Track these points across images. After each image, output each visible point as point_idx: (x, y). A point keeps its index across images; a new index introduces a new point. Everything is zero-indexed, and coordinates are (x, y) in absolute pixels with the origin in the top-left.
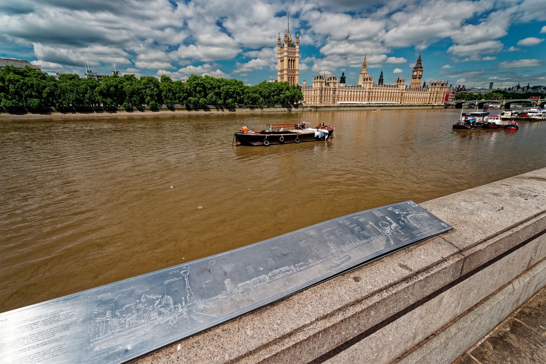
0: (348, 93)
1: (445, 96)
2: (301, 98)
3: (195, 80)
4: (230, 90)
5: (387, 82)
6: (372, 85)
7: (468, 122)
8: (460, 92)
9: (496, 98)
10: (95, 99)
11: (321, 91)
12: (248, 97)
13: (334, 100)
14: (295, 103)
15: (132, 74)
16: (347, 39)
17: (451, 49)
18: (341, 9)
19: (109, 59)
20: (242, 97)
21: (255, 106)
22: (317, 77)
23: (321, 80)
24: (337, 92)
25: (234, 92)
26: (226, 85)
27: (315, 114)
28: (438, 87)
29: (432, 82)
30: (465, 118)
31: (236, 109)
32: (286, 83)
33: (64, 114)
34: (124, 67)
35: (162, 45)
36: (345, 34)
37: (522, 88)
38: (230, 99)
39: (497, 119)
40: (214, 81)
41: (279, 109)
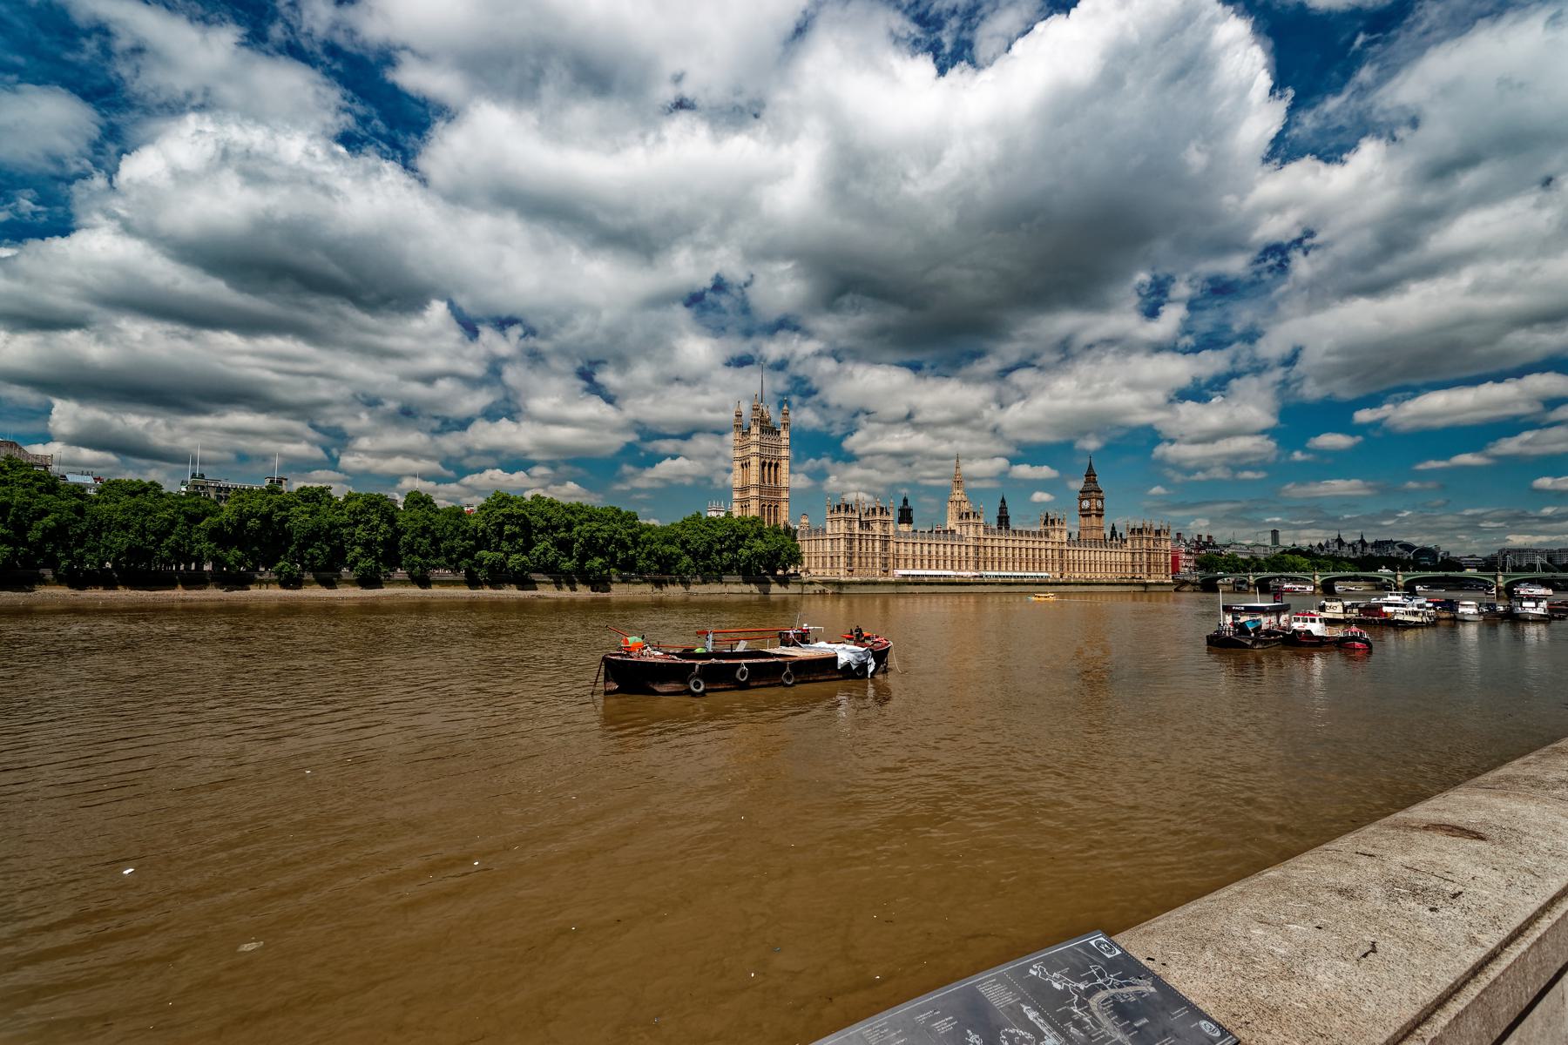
0: (922, 548)
1: (1170, 561)
2: (796, 558)
3: (504, 507)
4: (599, 534)
5: (1020, 524)
6: (981, 529)
7: (1242, 628)
8: (1204, 552)
9: (1294, 567)
10: (192, 549)
11: (851, 541)
12: (649, 555)
13: (886, 565)
14: (780, 572)
15: (324, 485)
16: (908, 419)
17: (1159, 450)
18: (890, 355)
19: (266, 445)
20: (630, 552)
21: (667, 577)
22: (839, 507)
23: (849, 515)
24: (892, 546)
25: (609, 541)
27: (835, 603)
28: (1148, 539)
29: (1131, 526)
30: (1233, 619)
31: (613, 587)
32: (755, 520)
33: (78, 592)
34: (303, 466)
35: (424, 417)
36: (903, 410)
37: (1349, 545)
38: (596, 558)
39: (1313, 621)
40: (557, 511)
41: (736, 588)
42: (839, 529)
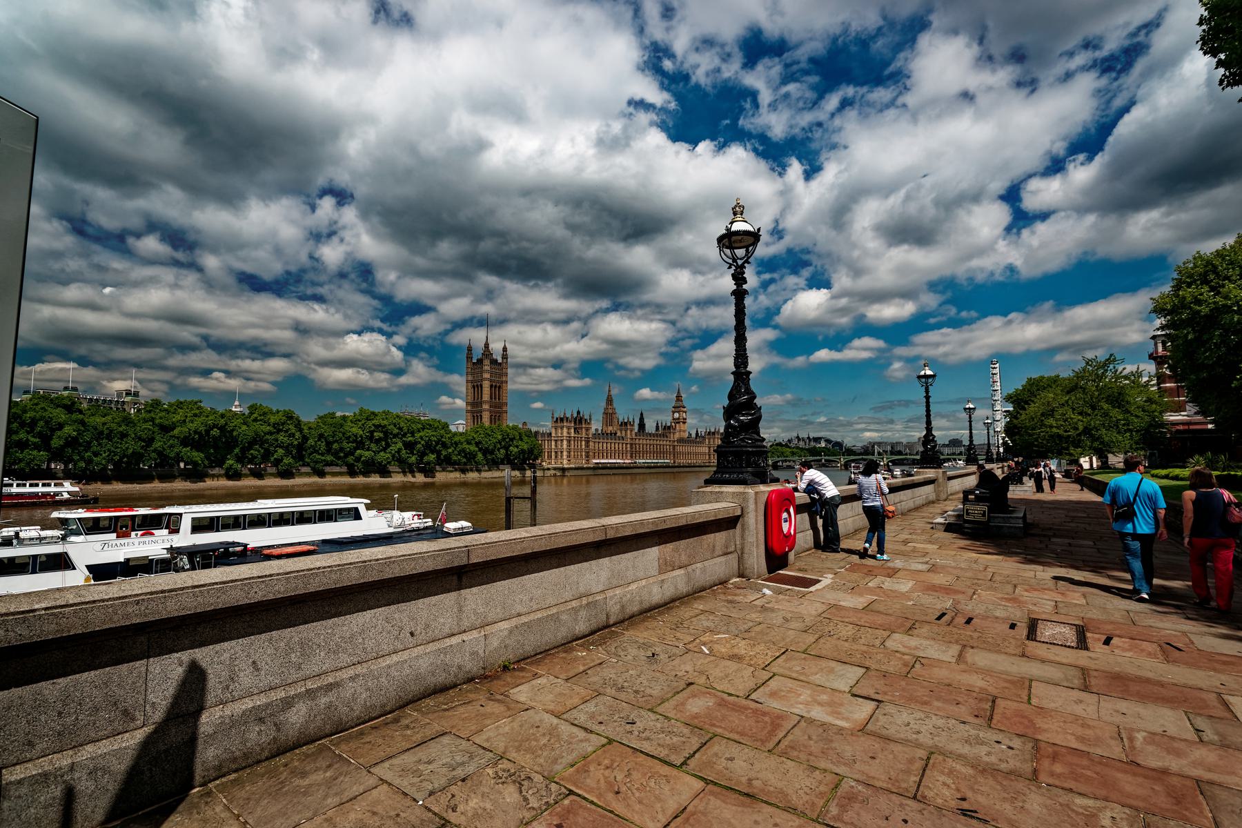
2: (540, 453)
3: (373, 419)
20: (450, 450)
21: (468, 467)
25: (437, 443)
26: (423, 429)
31: (437, 474)
42: (562, 433)
